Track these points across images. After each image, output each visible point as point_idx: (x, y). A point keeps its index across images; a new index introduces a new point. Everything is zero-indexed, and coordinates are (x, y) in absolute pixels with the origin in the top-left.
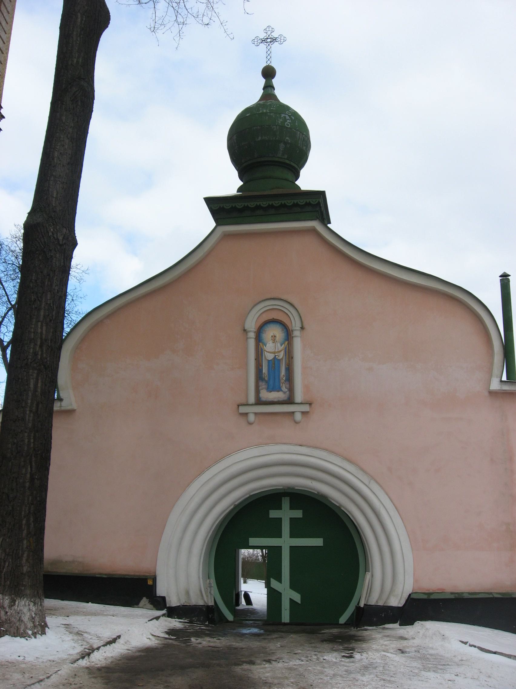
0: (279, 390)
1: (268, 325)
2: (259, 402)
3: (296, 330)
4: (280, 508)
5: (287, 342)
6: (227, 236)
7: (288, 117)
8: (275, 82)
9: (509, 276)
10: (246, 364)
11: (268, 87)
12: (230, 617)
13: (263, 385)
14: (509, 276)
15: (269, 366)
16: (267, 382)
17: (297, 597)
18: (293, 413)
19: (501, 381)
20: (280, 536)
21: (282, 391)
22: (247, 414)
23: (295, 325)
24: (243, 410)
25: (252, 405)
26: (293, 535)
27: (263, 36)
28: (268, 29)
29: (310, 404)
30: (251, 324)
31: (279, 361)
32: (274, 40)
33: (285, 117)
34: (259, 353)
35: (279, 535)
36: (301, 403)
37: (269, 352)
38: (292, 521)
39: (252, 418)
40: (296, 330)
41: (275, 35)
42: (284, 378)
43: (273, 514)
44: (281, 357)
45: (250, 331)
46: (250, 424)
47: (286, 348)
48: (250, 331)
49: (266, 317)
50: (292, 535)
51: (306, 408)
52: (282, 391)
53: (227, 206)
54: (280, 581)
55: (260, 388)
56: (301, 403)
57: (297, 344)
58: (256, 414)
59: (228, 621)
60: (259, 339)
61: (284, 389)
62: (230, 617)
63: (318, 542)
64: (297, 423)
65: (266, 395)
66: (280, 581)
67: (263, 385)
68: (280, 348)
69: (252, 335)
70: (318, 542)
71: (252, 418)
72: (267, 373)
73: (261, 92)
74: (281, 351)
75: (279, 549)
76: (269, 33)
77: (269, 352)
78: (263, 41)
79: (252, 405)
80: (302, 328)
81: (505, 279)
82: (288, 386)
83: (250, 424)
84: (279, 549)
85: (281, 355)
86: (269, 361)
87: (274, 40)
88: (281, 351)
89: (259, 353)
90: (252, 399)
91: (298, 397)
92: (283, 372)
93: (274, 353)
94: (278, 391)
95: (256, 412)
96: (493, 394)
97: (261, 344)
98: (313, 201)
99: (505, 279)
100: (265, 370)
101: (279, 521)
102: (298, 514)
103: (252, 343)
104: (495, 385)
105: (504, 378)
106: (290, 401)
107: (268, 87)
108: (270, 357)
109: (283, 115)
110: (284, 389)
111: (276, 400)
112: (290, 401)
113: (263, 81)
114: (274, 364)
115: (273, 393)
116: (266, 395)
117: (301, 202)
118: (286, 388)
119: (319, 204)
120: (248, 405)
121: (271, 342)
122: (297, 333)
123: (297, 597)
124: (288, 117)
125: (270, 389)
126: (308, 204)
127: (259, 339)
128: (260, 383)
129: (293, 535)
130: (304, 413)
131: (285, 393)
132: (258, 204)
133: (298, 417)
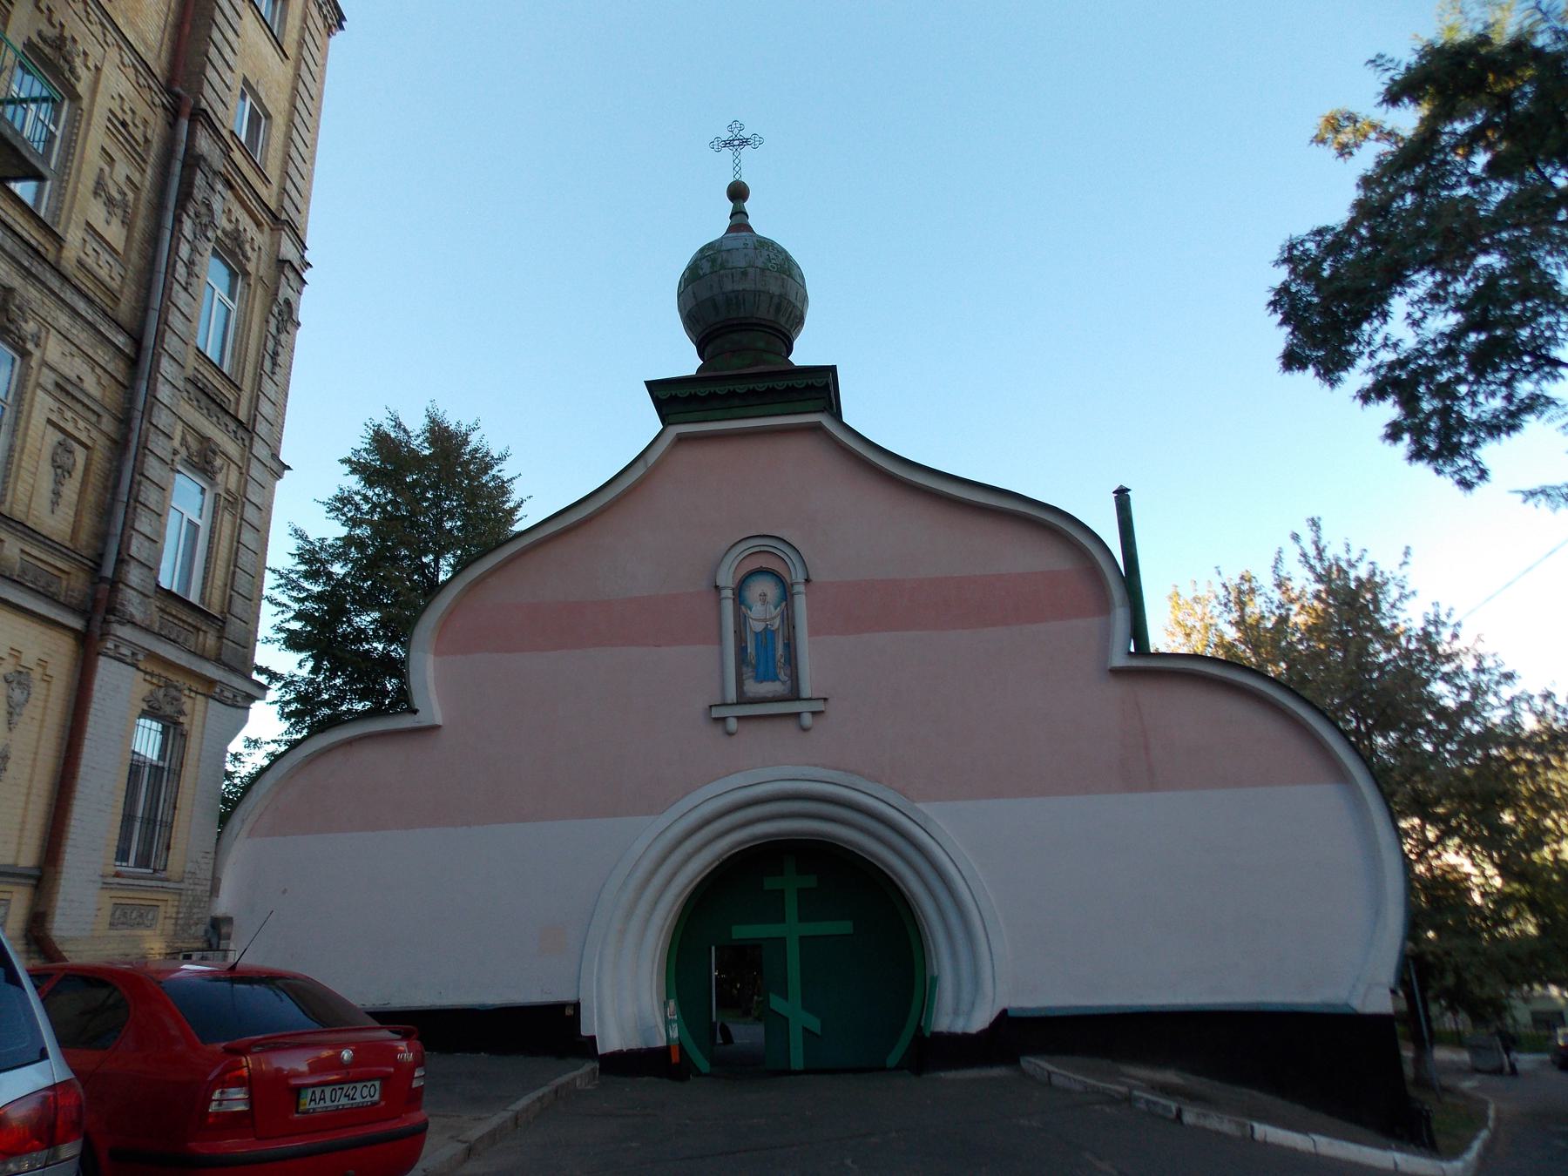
0: (775, 678)
1: (754, 578)
2: (743, 700)
3: (798, 583)
5: (784, 604)
6: (681, 439)
8: (748, 206)
9: (1129, 490)
10: (720, 641)
14: (1129, 490)
15: (757, 640)
16: (755, 668)
17: (815, 1025)
19: (1130, 653)
20: (782, 920)
21: (779, 680)
22: (724, 719)
24: (716, 713)
26: (802, 918)
27: (726, 136)
28: (734, 126)
30: (727, 578)
32: (744, 142)
34: (741, 621)
37: (755, 620)
39: (733, 725)
40: (798, 583)
41: (746, 134)
42: (782, 660)
43: (770, 883)
44: (776, 626)
45: (725, 588)
46: (730, 734)
47: (783, 612)
48: (725, 588)
52: (779, 680)
53: (684, 392)
54: (785, 996)
55: (744, 677)
57: (801, 603)
58: (739, 718)
59: (699, 1074)
61: (782, 676)
63: (844, 927)
64: (805, 730)
65: (754, 688)
66: (785, 996)
69: (728, 593)
70: (844, 927)
71: (733, 725)
72: (754, 653)
73: (728, 222)
74: (775, 617)
76: (736, 131)
77: (755, 620)
78: (728, 143)
80: (807, 581)
81: (1122, 496)
82: (788, 672)
83: (730, 734)
85: (777, 622)
86: (756, 634)
87: (744, 142)
88: (775, 617)
89: (741, 621)
90: (732, 695)
91: (806, 691)
92: (780, 650)
93: (765, 620)
94: (774, 681)
95: (741, 714)
96: (1118, 672)
97: (743, 607)
98: (818, 382)
99: (1122, 496)
100: (751, 649)
102: (810, 881)
103: (728, 606)
104: (1119, 661)
105: (1132, 650)
106: (794, 695)
108: (759, 627)
110: (782, 676)
111: (770, 695)
113: (729, 206)
114: (766, 636)
115: (764, 684)
116: (754, 688)
117: (800, 383)
118: (785, 675)
119: (827, 385)
120: (724, 704)
121: (759, 604)
122: (800, 588)
123: (815, 1025)
126: (810, 388)
128: (745, 669)
130: (814, 713)
131: (784, 683)
132: (731, 388)
133: (807, 720)
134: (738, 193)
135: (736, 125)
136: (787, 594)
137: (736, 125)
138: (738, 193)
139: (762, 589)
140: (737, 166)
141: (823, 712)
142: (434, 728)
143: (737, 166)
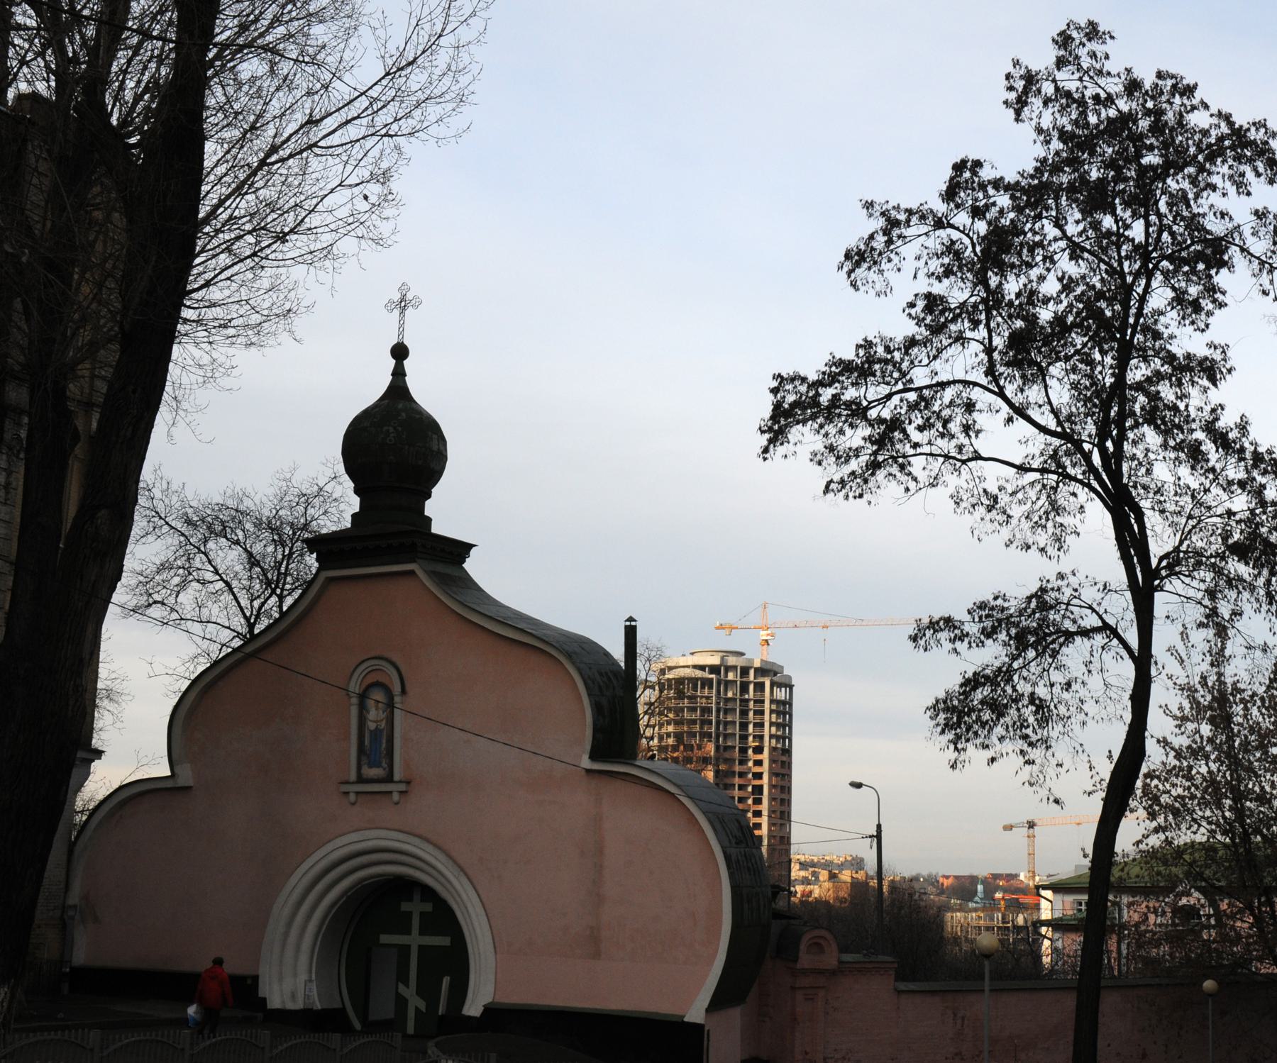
0: (379, 766)
2: (361, 780)
4: (410, 900)
7: (391, 430)
11: (399, 373)
12: (358, 1026)
13: (364, 760)
18: (391, 792)
20: (408, 932)
22: (348, 793)
23: (397, 689)
25: (353, 783)
26: (421, 933)
29: (408, 783)
30: (355, 687)
31: (381, 731)
33: (388, 431)
35: (408, 932)
36: (400, 782)
38: (422, 914)
39: (352, 797)
43: (405, 907)
49: (369, 680)
50: (408, 932)
51: (402, 787)
54: (407, 986)
56: (400, 782)
58: (357, 793)
60: (362, 707)
61: (384, 765)
62: (358, 1026)
66: (407, 986)
67: (364, 760)
68: (382, 715)
71: (352, 797)
75: (408, 947)
79: (353, 783)
80: (404, 692)
84: (408, 947)
85: (383, 725)
90: (353, 777)
91: (397, 777)
100: (367, 743)
101: (409, 915)
102: (428, 907)
103: (354, 711)
106: (389, 779)
107: (399, 373)
108: (372, 726)
109: (385, 428)
112: (389, 779)
114: (376, 734)
120: (347, 783)
124: (391, 430)
125: (371, 766)
127: (362, 707)
129: (421, 933)
130: (401, 792)
134: (400, 352)
135: (390, 306)
136: (390, 705)
137: (390, 306)
138: (400, 352)
139: (378, 695)
140: (401, 326)
141: (406, 792)
142: (188, 788)
143: (401, 326)
